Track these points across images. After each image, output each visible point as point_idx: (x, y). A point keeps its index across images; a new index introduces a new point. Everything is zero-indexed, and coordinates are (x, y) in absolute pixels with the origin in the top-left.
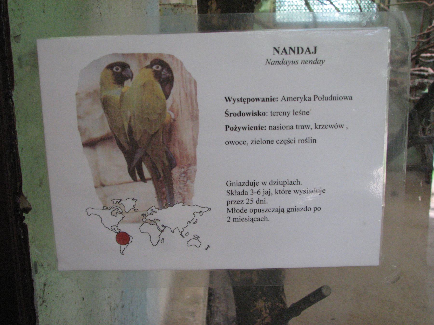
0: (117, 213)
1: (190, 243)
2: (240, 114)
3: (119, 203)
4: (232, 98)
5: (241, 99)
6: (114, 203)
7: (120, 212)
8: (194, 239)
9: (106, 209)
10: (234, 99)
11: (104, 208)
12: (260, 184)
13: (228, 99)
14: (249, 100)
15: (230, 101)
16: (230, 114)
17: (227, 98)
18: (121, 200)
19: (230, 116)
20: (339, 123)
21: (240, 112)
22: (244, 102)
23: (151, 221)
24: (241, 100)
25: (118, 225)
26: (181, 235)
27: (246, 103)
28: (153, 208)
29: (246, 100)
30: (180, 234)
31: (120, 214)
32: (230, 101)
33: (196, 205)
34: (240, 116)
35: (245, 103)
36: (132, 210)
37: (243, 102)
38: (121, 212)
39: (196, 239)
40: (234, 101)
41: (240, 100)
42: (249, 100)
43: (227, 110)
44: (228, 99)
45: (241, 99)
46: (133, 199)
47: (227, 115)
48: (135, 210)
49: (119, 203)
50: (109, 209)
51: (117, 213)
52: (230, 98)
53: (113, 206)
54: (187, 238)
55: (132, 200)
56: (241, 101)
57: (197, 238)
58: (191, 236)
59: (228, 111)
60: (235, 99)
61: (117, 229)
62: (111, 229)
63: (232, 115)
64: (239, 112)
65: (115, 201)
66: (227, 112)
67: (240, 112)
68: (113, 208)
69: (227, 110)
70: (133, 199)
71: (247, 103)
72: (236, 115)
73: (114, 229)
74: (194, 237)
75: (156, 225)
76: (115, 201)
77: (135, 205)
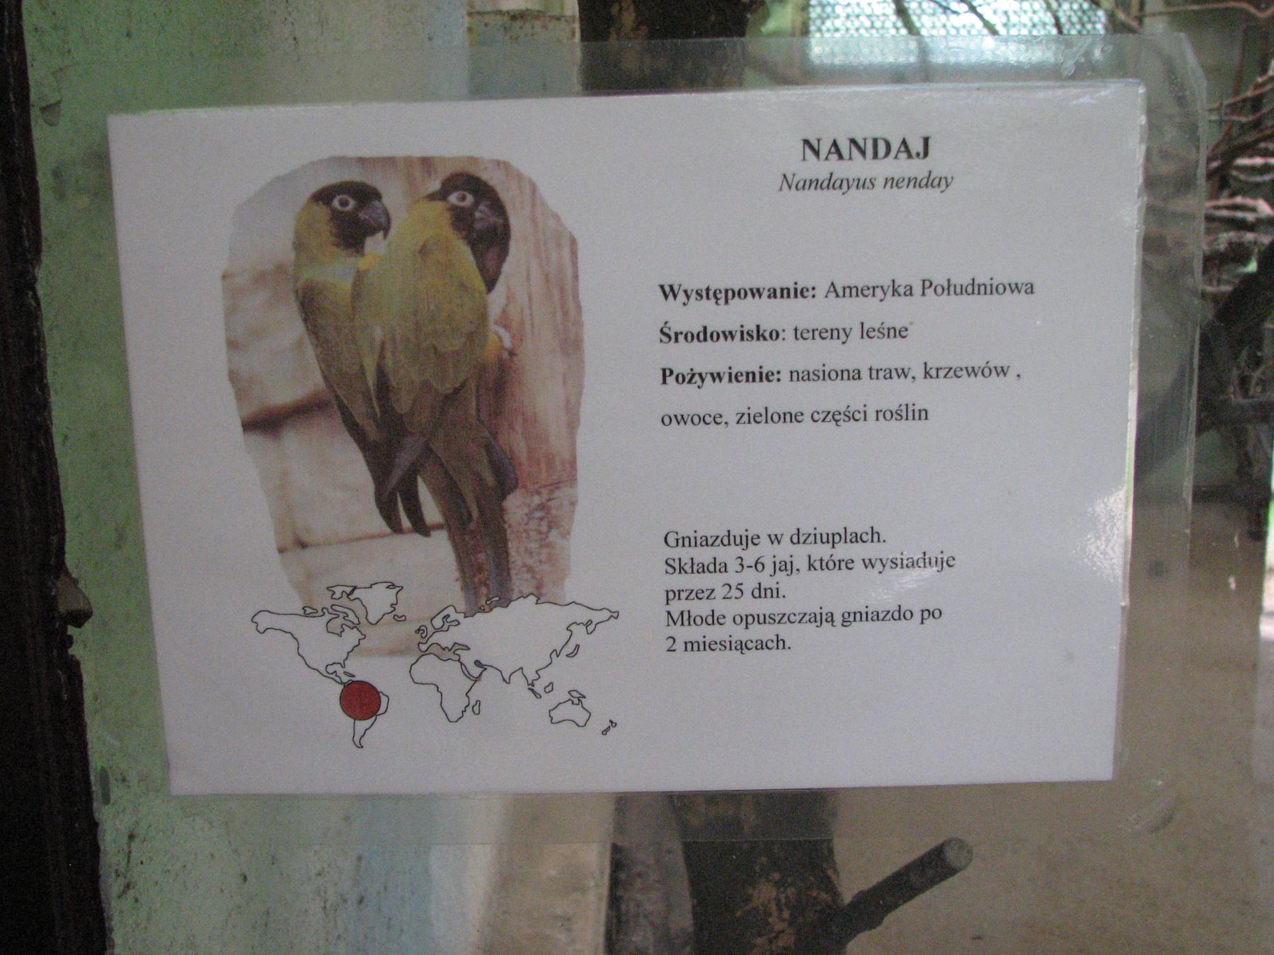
0: (342, 625)
2: (705, 335)
3: (348, 595)
4: (682, 288)
5: (708, 290)
6: (334, 596)
7: (352, 622)
9: (311, 613)
10: (686, 292)
11: (305, 611)
13: (669, 292)
15: (675, 296)
16: (676, 334)
17: (667, 289)
18: (355, 588)
19: (677, 340)
21: (705, 328)
22: (717, 299)
23: (444, 649)
24: (707, 294)
25: (346, 662)
27: (722, 301)
28: (450, 611)
29: (723, 295)
30: (529, 689)
31: (352, 629)
32: (675, 296)
33: (576, 603)
34: (705, 339)
35: (719, 302)
36: (389, 618)
37: (713, 300)
38: (356, 622)
40: (688, 297)
41: (704, 294)
43: (666, 323)
44: (669, 292)
45: (708, 290)
46: (392, 586)
47: (665, 339)
48: (396, 617)
49: (348, 595)
50: (320, 613)
51: (344, 626)
52: (676, 288)
53: (330, 605)
55: (387, 587)
56: (708, 298)
59: (668, 325)
60: (689, 292)
61: (345, 672)
62: (327, 672)
63: (681, 338)
64: (702, 329)
65: (338, 591)
66: (666, 330)
67: (705, 328)
68: (331, 611)
69: (666, 323)
70: (392, 586)
71: (727, 302)
72: (693, 339)
73: (335, 672)
75: (459, 660)
76: (338, 591)
77: (395, 602)
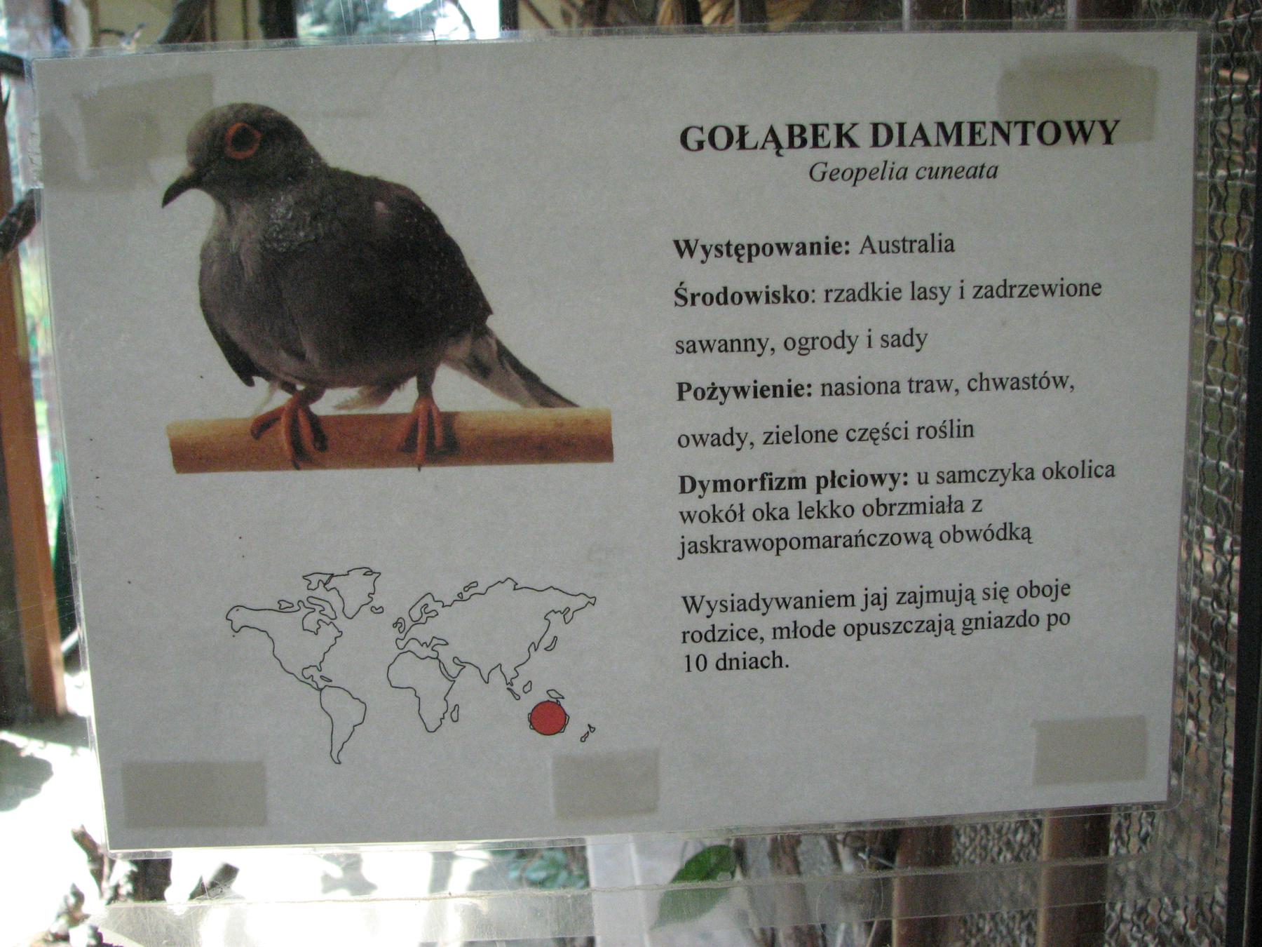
2: (724, 297)
5: (728, 245)
10: (704, 247)
13: (684, 248)
15: (692, 253)
16: (693, 296)
19: (693, 303)
21: (725, 289)
22: (739, 256)
27: (745, 258)
32: (692, 253)
35: (741, 259)
40: (707, 254)
44: (684, 248)
45: (728, 245)
47: (681, 302)
52: (692, 244)
56: (729, 254)
59: (683, 286)
63: (698, 300)
67: (725, 289)
71: (750, 260)
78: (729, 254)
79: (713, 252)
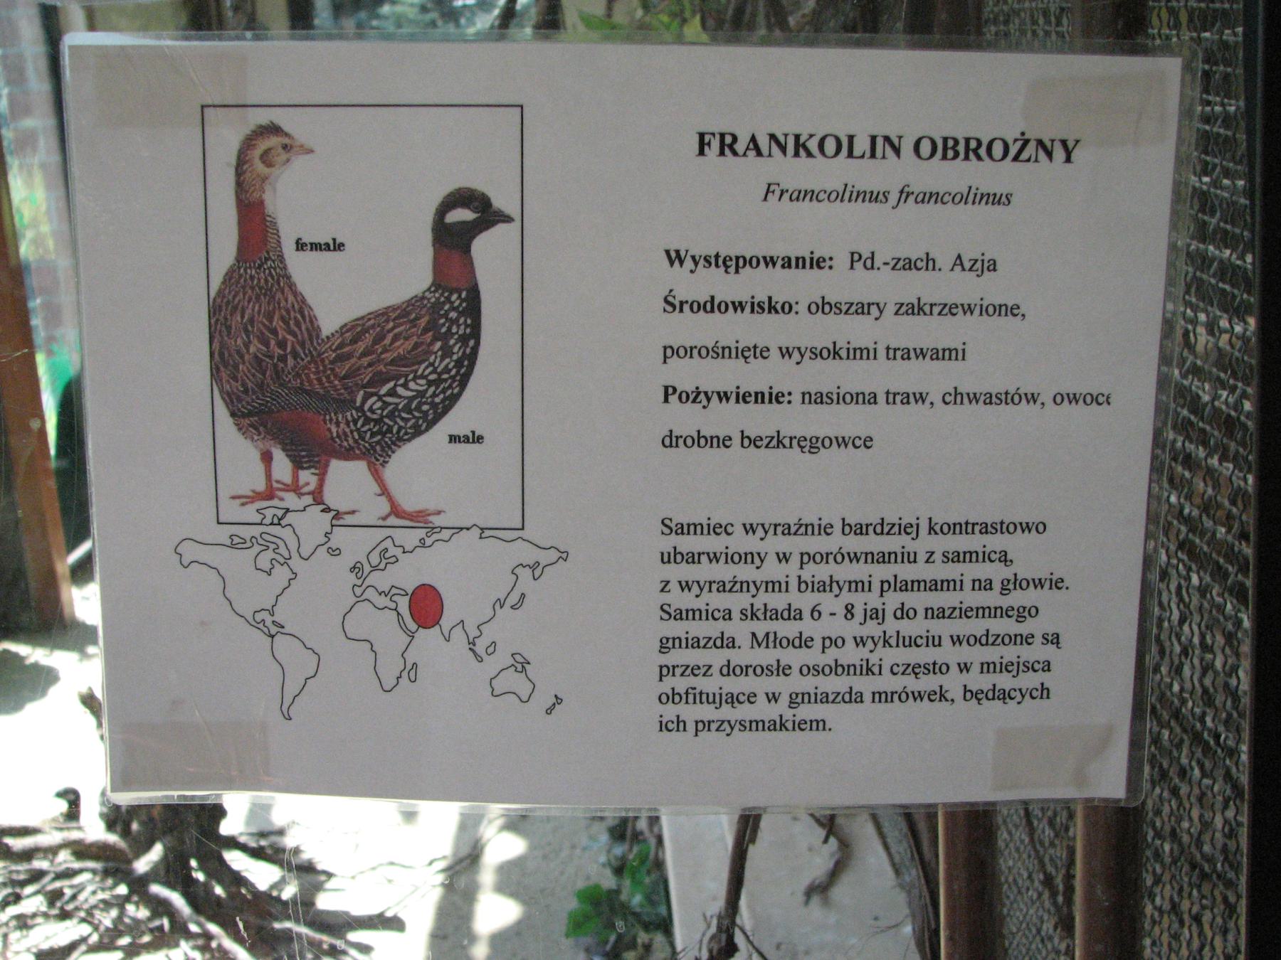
1: (499, 685)
4: (689, 254)
5: (717, 256)
8: (513, 668)
10: (693, 257)
12: (739, 530)
13: (675, 258)
14: (740, 263)
15: (681, 263)
16: (682, 303)
17: (673, 255)
19: (681, 311)
20: (1027, 388)
26: (471, 653)
32: (681, 263)
39: (520, 668)
40: (696, 264)
41: (713, 261)
42: (740, 263)
43: (671, 291)
44: (675, 258)
45: (717, 256)
52: (683, 254)
54: (493, 664)
56: (717, 266)
57: (521, 665)
58: (502, 658)
59: (672, 294)
60: (697, 258)
63: (686, 307)
66: (670, 299)
69: (671, 291)
74: (512, 662)
78: (717, 266)
79: (702, 262)
